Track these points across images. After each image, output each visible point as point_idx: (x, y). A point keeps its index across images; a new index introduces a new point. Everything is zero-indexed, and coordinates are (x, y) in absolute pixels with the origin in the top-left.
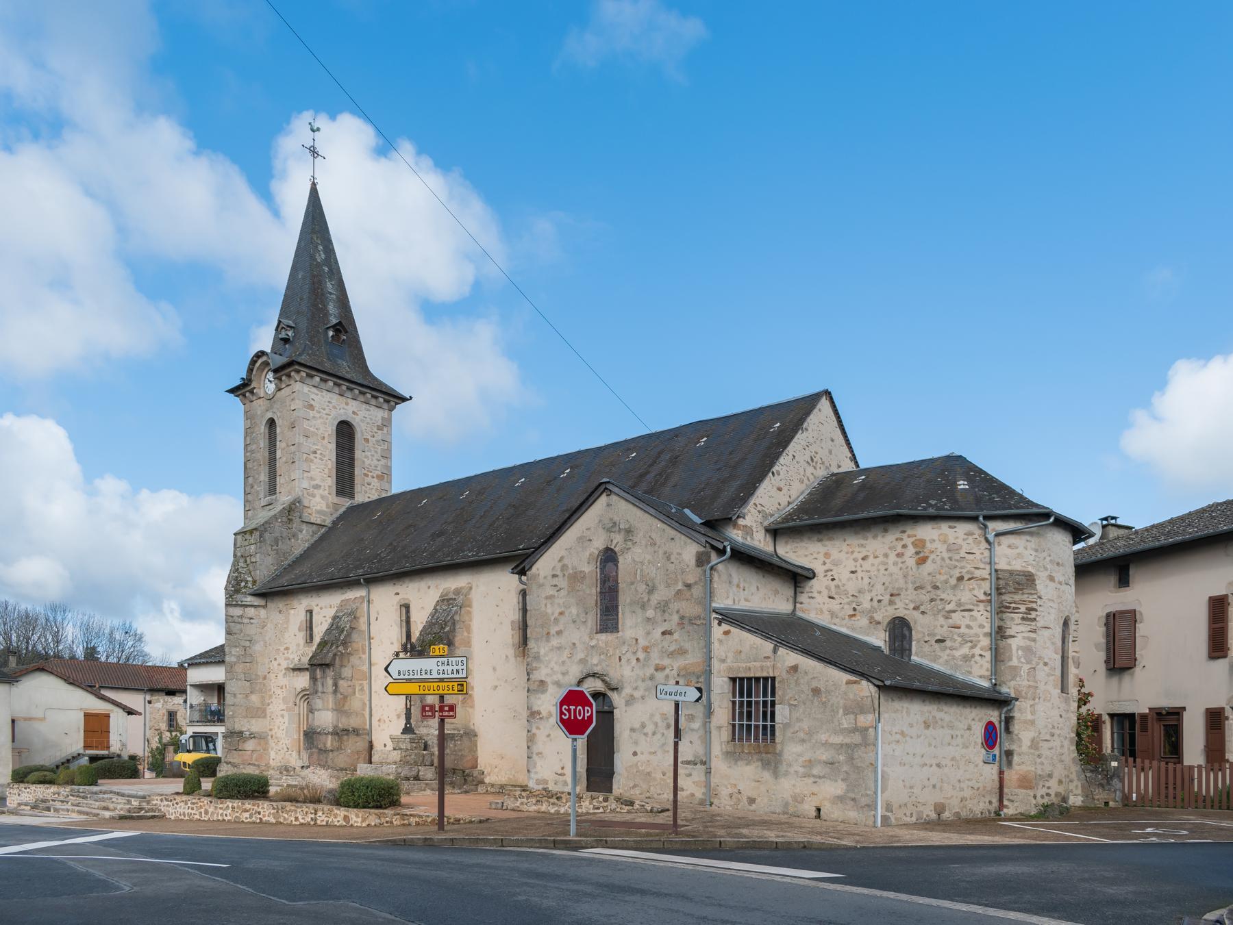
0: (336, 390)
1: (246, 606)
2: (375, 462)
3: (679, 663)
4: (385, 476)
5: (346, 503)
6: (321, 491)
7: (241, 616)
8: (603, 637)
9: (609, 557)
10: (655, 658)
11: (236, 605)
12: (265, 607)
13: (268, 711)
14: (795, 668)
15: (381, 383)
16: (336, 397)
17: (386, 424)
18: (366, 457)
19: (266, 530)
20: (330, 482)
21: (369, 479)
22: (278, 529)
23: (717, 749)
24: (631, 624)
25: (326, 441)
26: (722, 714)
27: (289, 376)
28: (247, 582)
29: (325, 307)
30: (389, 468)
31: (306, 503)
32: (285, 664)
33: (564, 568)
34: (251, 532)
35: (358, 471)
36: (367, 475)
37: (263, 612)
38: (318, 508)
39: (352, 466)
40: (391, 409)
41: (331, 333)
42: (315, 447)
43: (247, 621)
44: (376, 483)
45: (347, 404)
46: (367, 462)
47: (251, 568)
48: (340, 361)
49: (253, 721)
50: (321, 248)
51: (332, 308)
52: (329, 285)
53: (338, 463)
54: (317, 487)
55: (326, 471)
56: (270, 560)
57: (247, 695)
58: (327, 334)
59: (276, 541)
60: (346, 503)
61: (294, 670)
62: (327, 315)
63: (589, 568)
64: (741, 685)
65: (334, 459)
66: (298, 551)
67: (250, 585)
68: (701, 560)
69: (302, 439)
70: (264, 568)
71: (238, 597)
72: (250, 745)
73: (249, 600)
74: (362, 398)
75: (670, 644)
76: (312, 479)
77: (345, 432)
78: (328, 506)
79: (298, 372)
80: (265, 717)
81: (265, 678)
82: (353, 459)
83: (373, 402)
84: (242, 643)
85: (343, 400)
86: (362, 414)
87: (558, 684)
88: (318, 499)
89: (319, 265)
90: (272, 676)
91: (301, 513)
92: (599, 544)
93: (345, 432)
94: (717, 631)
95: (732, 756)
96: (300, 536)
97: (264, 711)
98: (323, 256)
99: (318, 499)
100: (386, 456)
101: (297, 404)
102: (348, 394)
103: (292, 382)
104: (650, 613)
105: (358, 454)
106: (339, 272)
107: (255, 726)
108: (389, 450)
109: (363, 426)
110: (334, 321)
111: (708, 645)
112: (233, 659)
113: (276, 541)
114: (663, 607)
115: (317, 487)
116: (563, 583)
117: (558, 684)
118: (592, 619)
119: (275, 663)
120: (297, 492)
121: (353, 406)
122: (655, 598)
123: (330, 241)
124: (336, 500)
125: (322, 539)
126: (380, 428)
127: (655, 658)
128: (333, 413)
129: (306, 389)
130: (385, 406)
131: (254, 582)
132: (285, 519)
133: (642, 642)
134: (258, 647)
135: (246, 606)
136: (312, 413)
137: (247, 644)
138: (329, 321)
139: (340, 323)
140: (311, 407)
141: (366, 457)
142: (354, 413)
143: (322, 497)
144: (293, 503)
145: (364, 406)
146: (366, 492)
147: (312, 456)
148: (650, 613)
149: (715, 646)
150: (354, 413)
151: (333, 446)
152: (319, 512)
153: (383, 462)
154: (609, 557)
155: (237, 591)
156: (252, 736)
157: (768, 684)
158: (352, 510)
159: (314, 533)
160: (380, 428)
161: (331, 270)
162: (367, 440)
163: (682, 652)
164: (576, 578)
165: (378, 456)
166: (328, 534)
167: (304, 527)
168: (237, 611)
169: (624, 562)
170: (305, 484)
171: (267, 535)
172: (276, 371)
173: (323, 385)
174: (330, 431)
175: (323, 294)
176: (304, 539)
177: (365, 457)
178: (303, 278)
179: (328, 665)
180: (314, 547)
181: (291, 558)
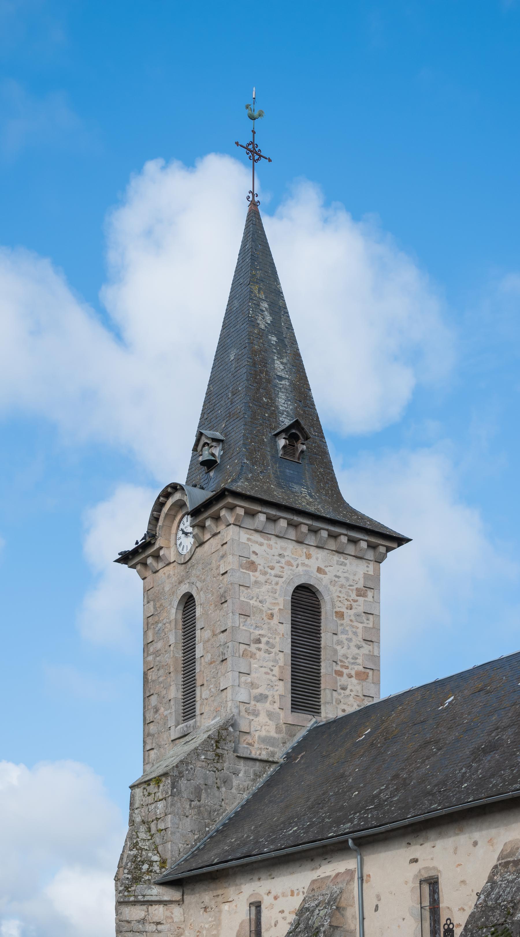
0: (292, 534)
1: (151, 903)
2: (354, 651)
4: (370, 672)
5: (309, 722)
6: (268, 705)
7: (143, 921)
11: (135, 903)
12: (180, 902)
15: (363, 517)
16: (290, 546)
17: (371, 585)
18: (339, 643)
19: (181, 775)
20: (283, 689)
21: (343, 680)
22: (200, 770)
25: (275, 620)
27: (217, 518)
28: (151, 863)
29: (273, 400)
30: (375, 659)
31: (244, 727)
34: (158, 780)
35: (325, 668)
36: (340, 674)
37: (177, 911)
38: (263, 733)
39: (316, 659)
40: (379, 560)
41: (282, 442)
42: (257, 632)
43: (153, 927)
44: (354, 685)
45: (309, 556)
46: (341, 651)
47: (158, 839)
48: (296, 488)
50: (265, 305)
51: (284, 403)
52: (278, 365)
53: (294, 656)
54: (262, 698)
55: (276, 670)
56: (187, 824)
58: (275, 444)
59: (198, 792)
60: (309, 722)
62: (275, 413)
65: (288, 650)
66: (232, 807)
67: (156, 868)
69: (237, 620)
70: (178, 840)
71: (138, 888)
73: (156, 892)
74: (332, 545)
76: (253, 685)
77: (305, 602)
78: (278, 730)
79: (231, 508)
82: (318, 648)
83: (351, 549)
85: (302, 550)
86: (331, 572)
88: (263, 718)
89: (262, 334)
91: (237, 742)
93: (305, 602)
96: (235, 782)
98: (269, 319)
99: (263, 718)
100: (371, 640)
101: (231, 563)
102: (311, 540)
103: (222, 527)
105: (326, 639)
106: (294, 342)
108: (376, 629)
109: (335, 591)
110: (287, 422)
113: (198, 792)
115: (262, 698)
120: (230, 709)
121: (319, 558)
123: (279, 293)
124: (292, 718)
125: (270, 783)
126: (360, 593)
128: (287, 573)
129: (244, 536)
130: (370, 554)
131: (163, 862)
135: (151, 903)
136: (253, 576)
138: (278, 423)
139: (296, 424)
140: (252, 566)
141: (339, 643)
142: (319, 570)
143: (270, 715)
144: (224, 727)
145: (336, 558)
146: (339, 701)
147: (253, 648)
150: (319, 570)
151: (286, 629)
153: (366, 648)
155: (136, 880)
158: (317, 732)
159: (257, 776)
160: (360, 593)
161: (281, 340)
162: (340, 615)
165: (358, 640)
166: (280, 775)
167: (242, 766)
168: (136, 913)
170: (243, 695)
171: (183, 783)
172: (195, 513)
173: (270, 528)
174: (281, 602)
175: (269, 381)
176: (243, 784)
177: (338, 642)
178: (238, 359)
180: (258, 797)
181: (222, 819)
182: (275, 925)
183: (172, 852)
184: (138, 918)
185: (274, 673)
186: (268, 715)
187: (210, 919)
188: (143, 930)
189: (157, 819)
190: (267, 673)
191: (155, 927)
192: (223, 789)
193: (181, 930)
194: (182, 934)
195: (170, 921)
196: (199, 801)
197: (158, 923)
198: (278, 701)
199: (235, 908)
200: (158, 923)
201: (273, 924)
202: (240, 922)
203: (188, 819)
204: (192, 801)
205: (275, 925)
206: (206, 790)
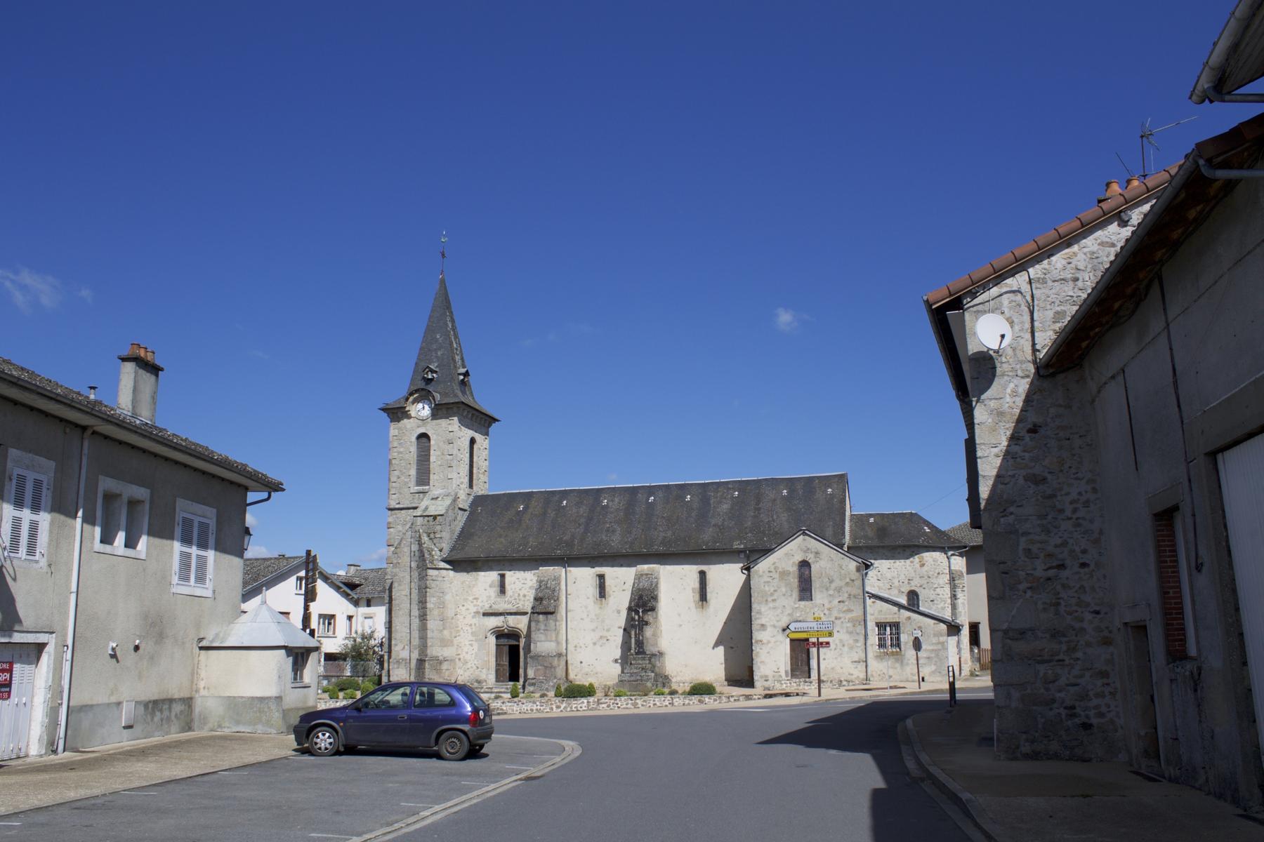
3: (850, 615)
8: (803, 603)
9: (804, 565)
10: (835, 613)
14: (909, 618)
23: (870, 655)
24: (819, 596)
26: (874, 639)
33: (776, 568)
61: (484, 614)
63: (794, 569)
64: (881, 626)
68: (858, 570)
72: (445, 666)
73: (443, 565)
75: (844, 607)
87: (774, 626)
92: (799, 557)
94: (869, 601)
95: (879, 657)
104: (831, 592)
111: (865, 608)
114: (839, 590)
116: (777, 576)
117: (774, 626)
118: (796, 594)
122: (833, 586)
127: (835, 613)
133: (827, 606)
134: (448, 597)
148: (831, 592)
149: (868, 608)
154: (804, 565)
157: (896, 625)
163: (850, 611)
164: (784, 574)
169: (815, 568)
179: (552, 613)
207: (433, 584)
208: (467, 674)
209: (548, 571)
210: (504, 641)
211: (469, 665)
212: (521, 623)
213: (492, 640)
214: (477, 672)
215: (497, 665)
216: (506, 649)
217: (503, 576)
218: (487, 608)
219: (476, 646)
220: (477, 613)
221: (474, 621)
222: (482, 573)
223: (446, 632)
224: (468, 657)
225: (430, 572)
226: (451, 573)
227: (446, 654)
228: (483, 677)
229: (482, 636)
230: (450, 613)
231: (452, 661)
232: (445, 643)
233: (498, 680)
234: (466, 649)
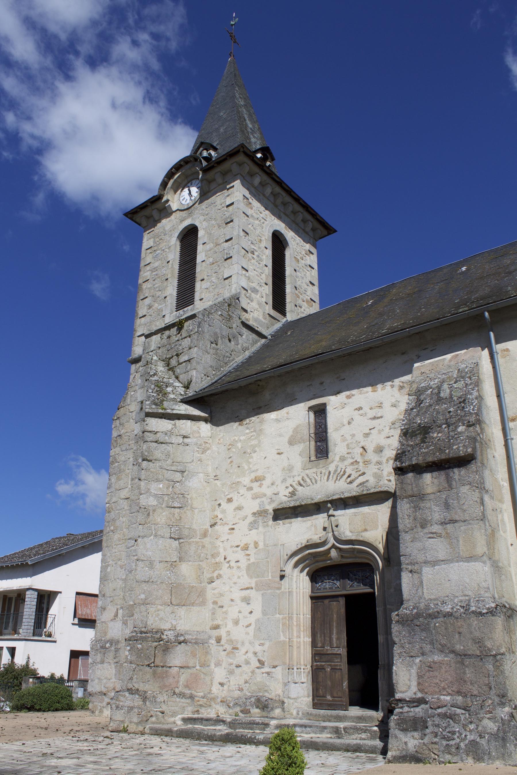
13: (210, 593)
32: (254, 506)
43: (180, 440)
49: (182, 611)
57: (173, 565)
72: (178, 657)
80: (203, 603)
81: (205, 535)
83: (302, 225)
84: (169, 475)
90: (221, 530)
97: (202, 593)
107: (187, 620)
112: (152, 502)
119: (229, 508)
132: (225, 314)
134: (195, 483)
137: (178, 476)
152: (256, 320)
156: (181, 641)
182: (349, 423)
183: (196, 378)
184: (164, 429)
185: (262, 277)
186: (259, 304)
187: (248, 431)
188: (169, 441)
189: (177, 355)
190: (257, 275)
191: (181, 439)
192: (233, 343)
193: (207, 445)
194: (208, 449)
195: (197, 435)
196: (217, 345)
197: (184, 437)
198: (265, 297)
199: (286, 415)
200: (184, 437)
201: (346, 422)
202: (295, 427)
203: (209, 356)
204: (212, 343)
205: (349, 423)
206: (221, 339)
207: (158, 452)
208: (237, 680)
209: (436, 368)
210: (330, 586)
211: (240, 657)
212: (369, 526)
213: (300, 584)
214: (260, 677)
215: (318, 655)
216: (338, 609)
217: (320, 412)
218: (283, 499)
219: (257, 605)
220: (261, 513)
221: (254, 535)
222: (273, 415)
223: (186, 569)
224: (239, 633)
225: (154, 424)
226: (205, 428)
227: (183, 626)
228: (275, 690)
229: (272, 575)
230: (198, 520)
231: (199, 643)
232: (182, 596)
233: (318, 701)
234: (233, 613)
